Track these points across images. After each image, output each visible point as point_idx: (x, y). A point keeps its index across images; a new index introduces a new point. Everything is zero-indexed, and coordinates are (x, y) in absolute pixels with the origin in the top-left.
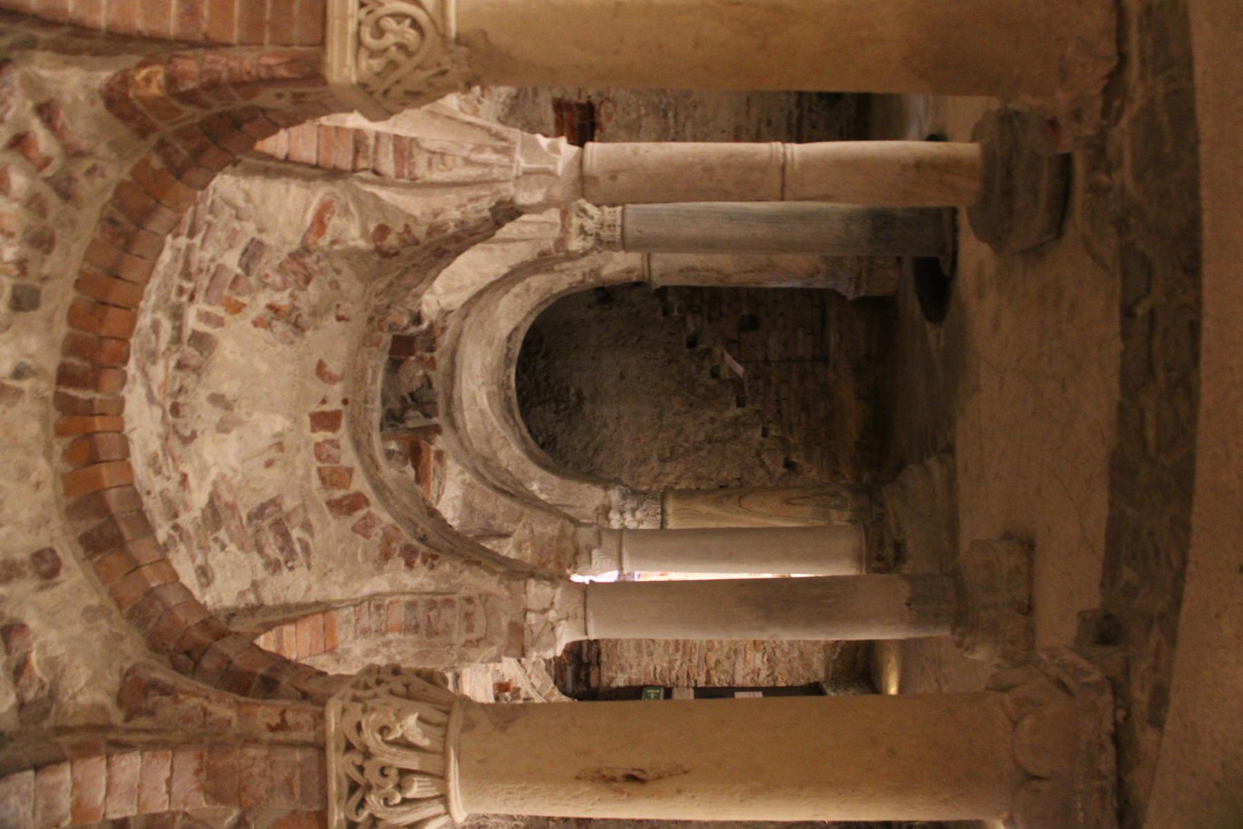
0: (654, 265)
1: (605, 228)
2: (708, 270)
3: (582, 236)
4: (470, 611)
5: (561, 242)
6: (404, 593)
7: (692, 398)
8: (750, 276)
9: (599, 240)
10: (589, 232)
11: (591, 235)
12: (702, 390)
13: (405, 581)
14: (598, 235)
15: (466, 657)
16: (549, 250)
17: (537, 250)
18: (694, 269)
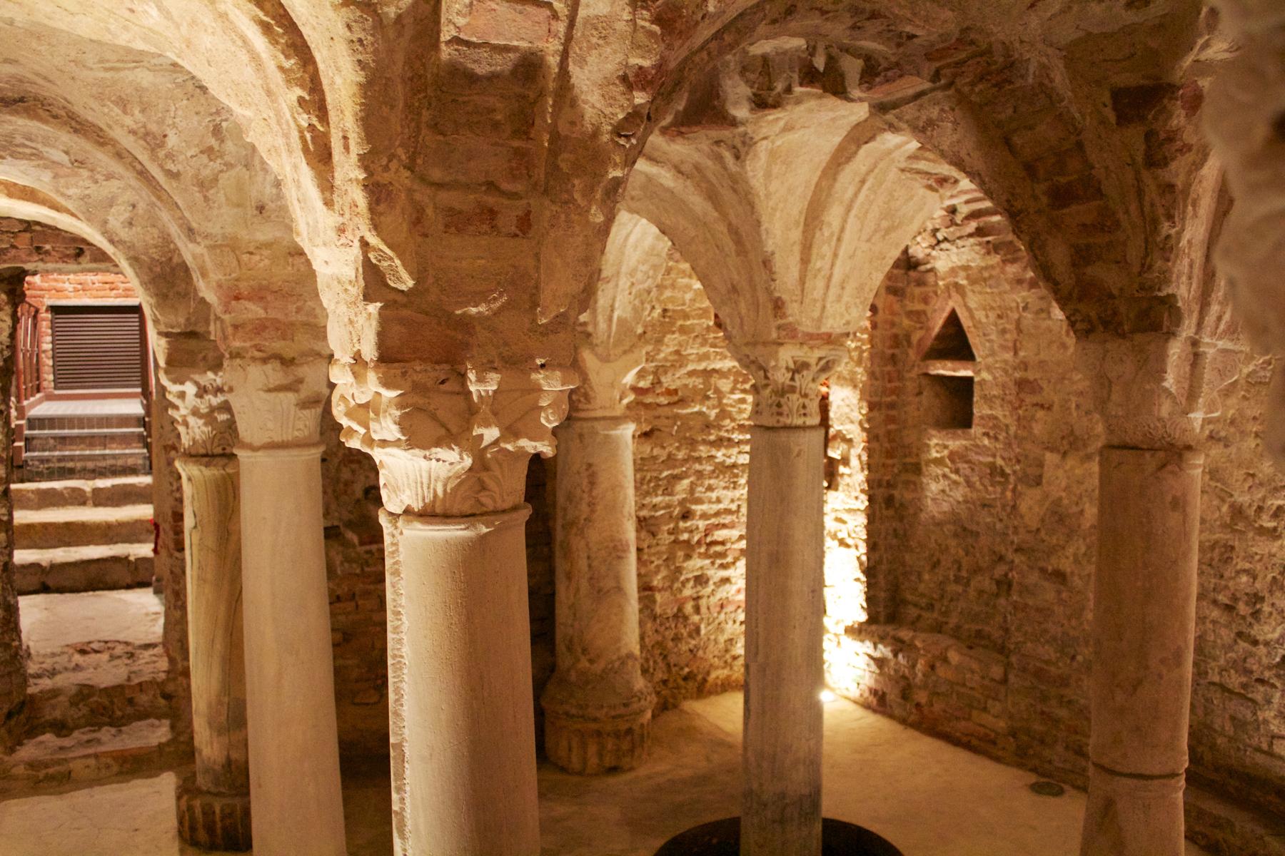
0: (596, 424)
1: (801, 400)
2: (591, 505)
3: (792, 365)
4: (500, 221)
5: (790, 332)
6: (565, 55)
7: (336, 461)
8: (583, 564)
9: (783, 391)
10: (797, 377)
11: (792, 379)
12: (346, 474)
13: (592, 58)
14: (792, 389)
15: (381, 208)
16: (784, 316)
17: (785, 297)
18: (592, 484)
